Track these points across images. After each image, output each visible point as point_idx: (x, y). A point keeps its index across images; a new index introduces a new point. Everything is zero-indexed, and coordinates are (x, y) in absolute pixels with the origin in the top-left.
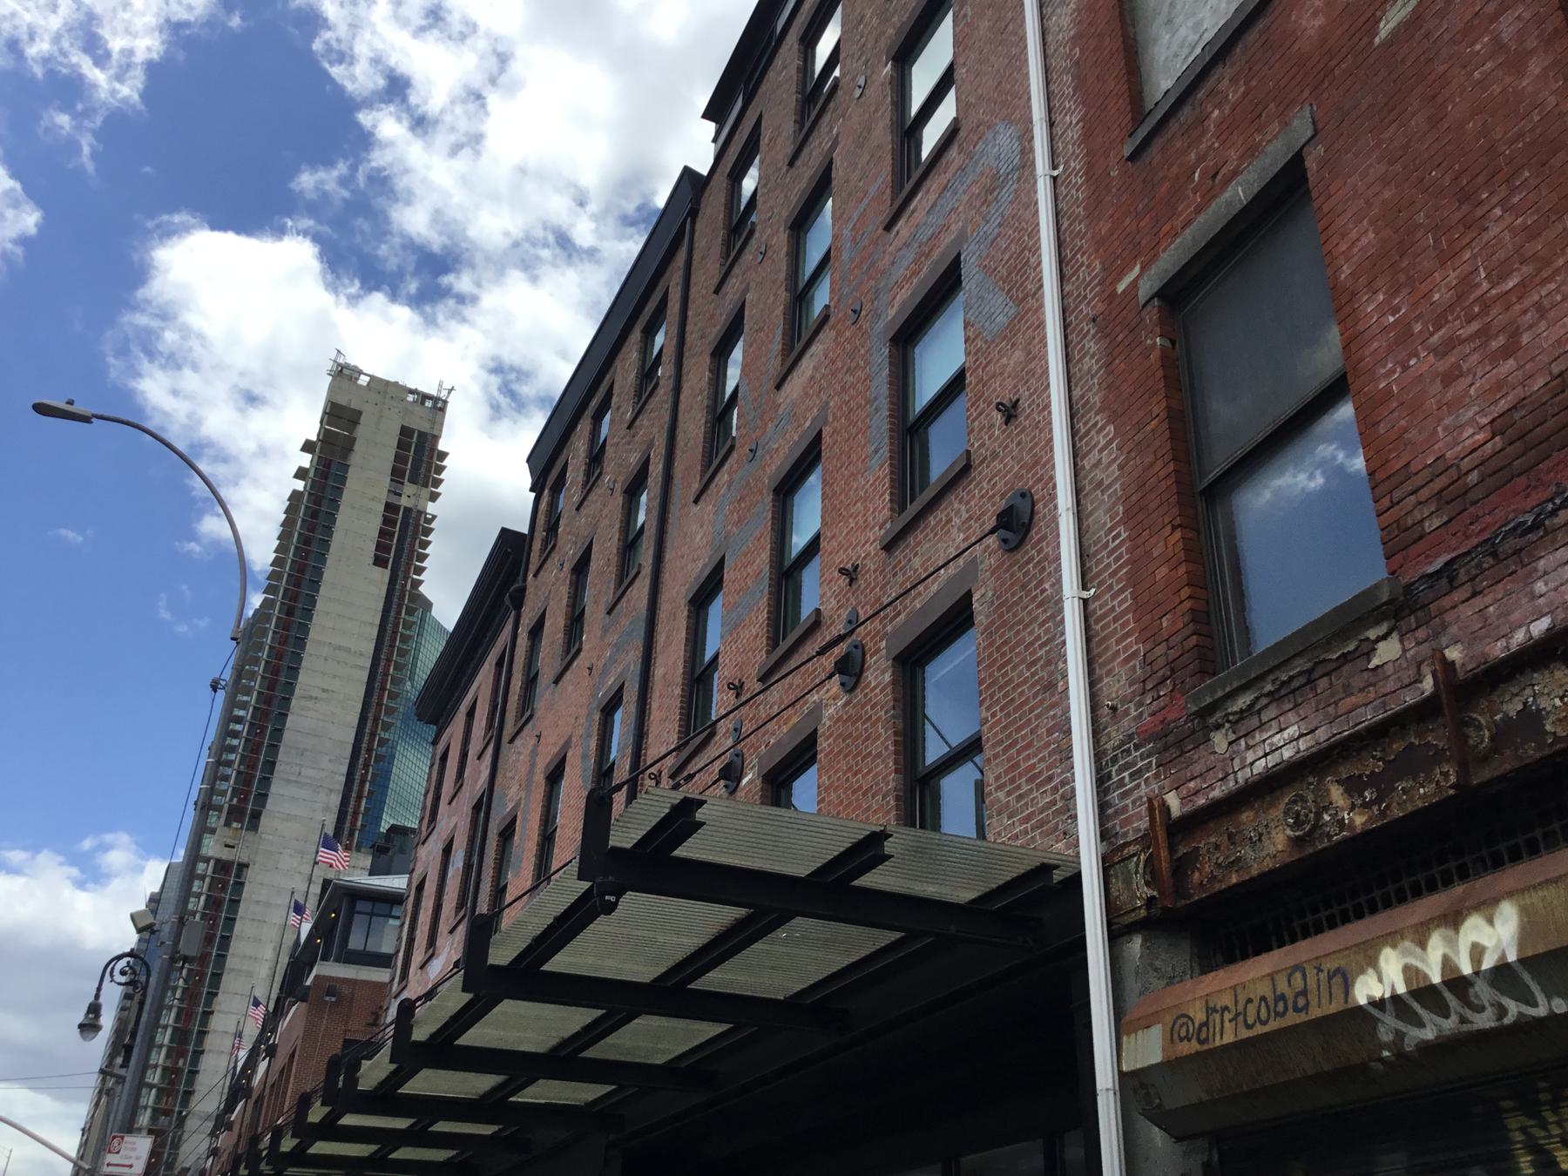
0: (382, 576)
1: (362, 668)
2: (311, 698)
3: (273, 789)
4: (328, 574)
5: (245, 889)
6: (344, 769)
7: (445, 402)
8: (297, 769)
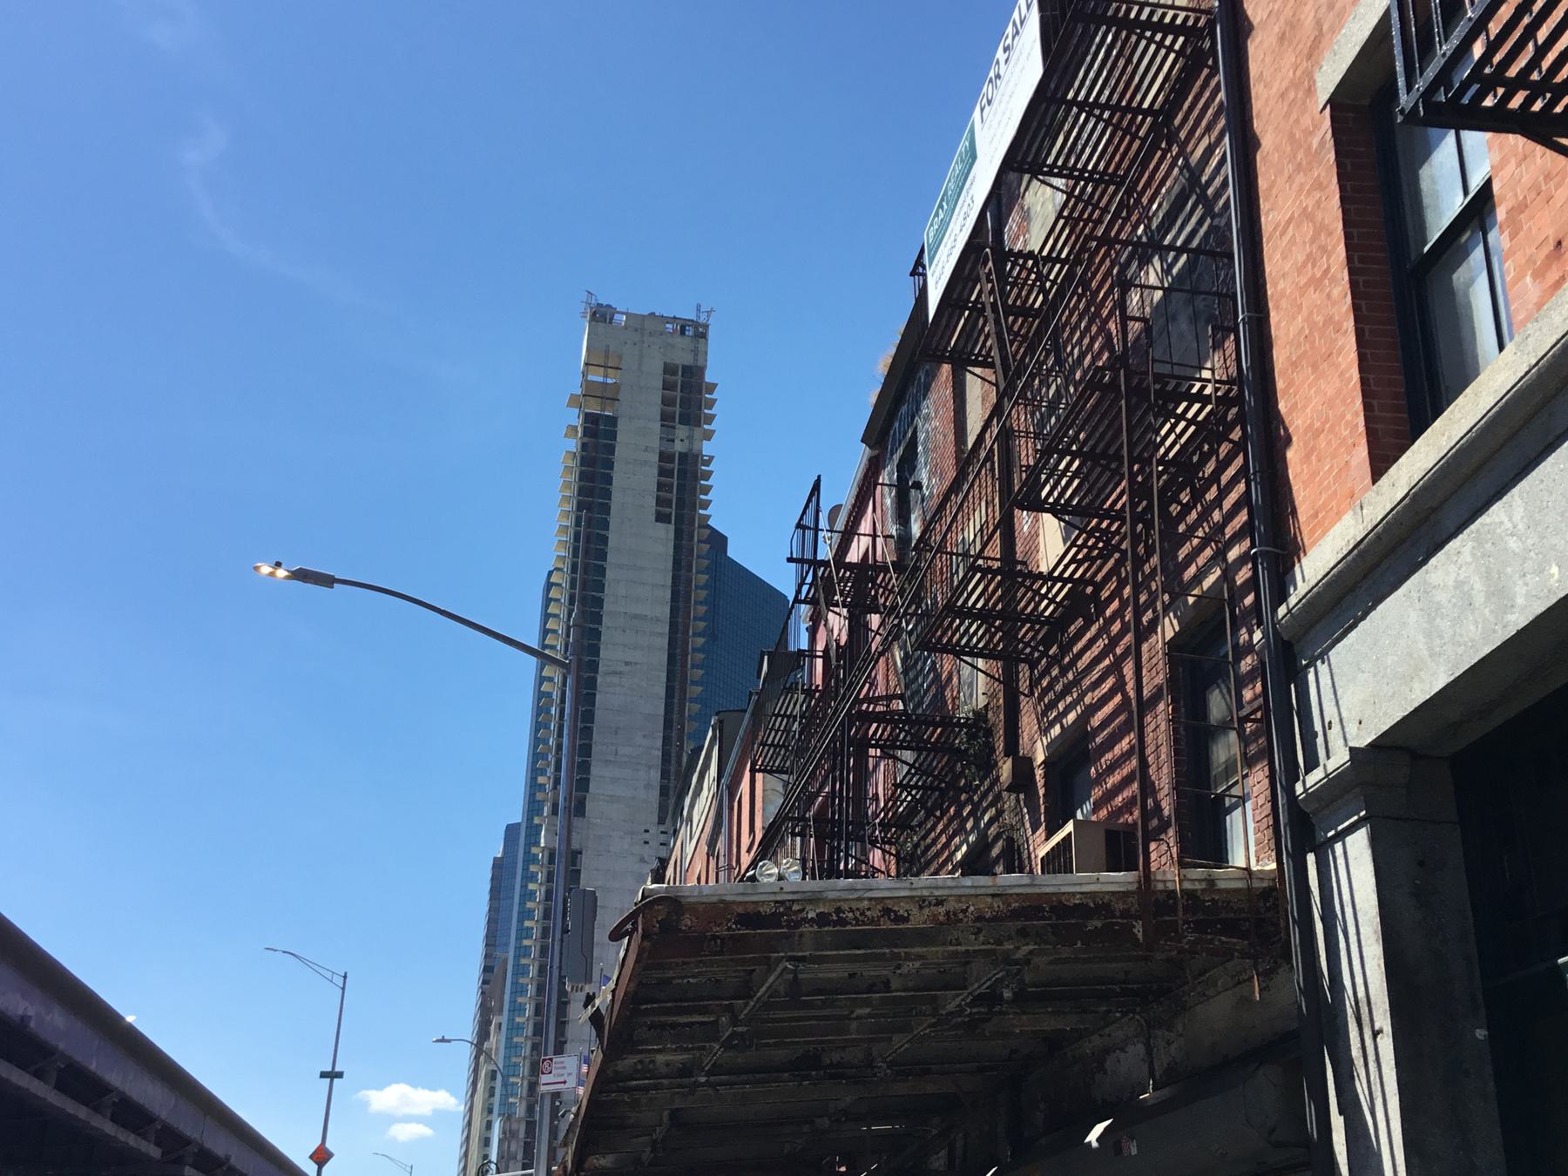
0: (666, 532)
1: (661, 634)
2: (616, 673)
3: (594, 770)
5: (582, 876)
6: (659, 743)
7: (706, 326)
8: (614, 748)
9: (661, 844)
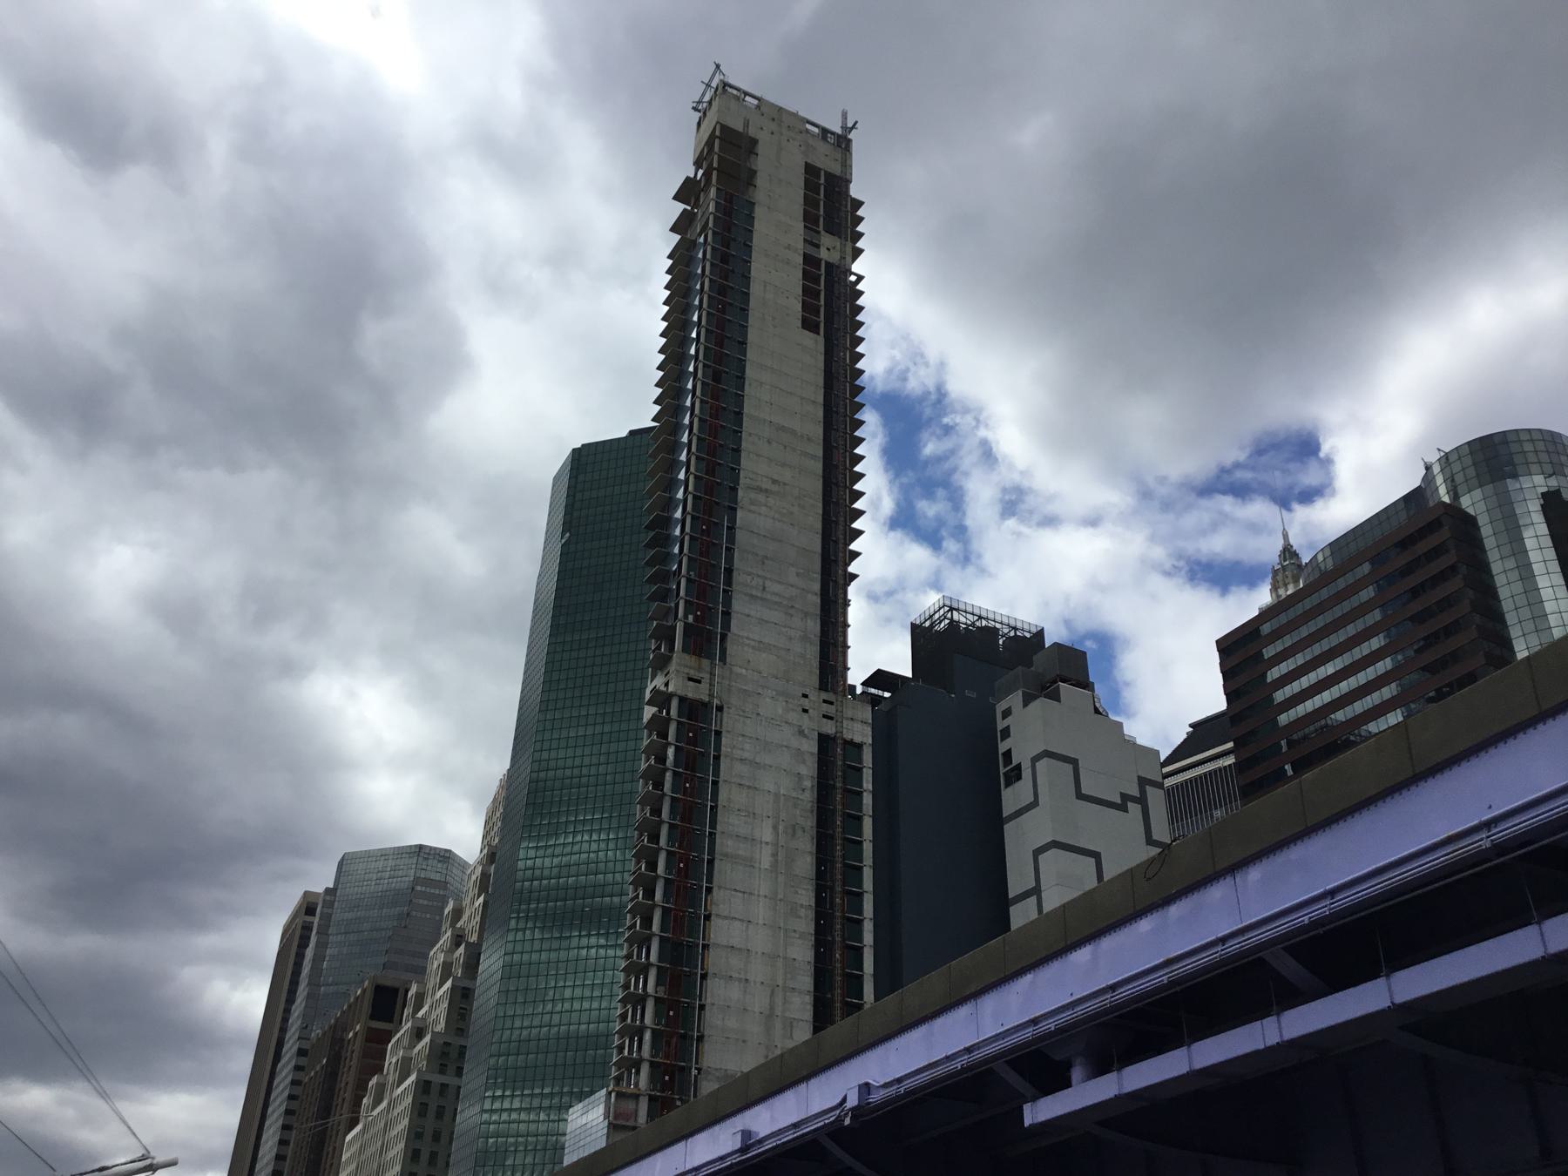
1: (814, 457)
2: (760, 490)
4: (753, 336)
9: (824, 716)
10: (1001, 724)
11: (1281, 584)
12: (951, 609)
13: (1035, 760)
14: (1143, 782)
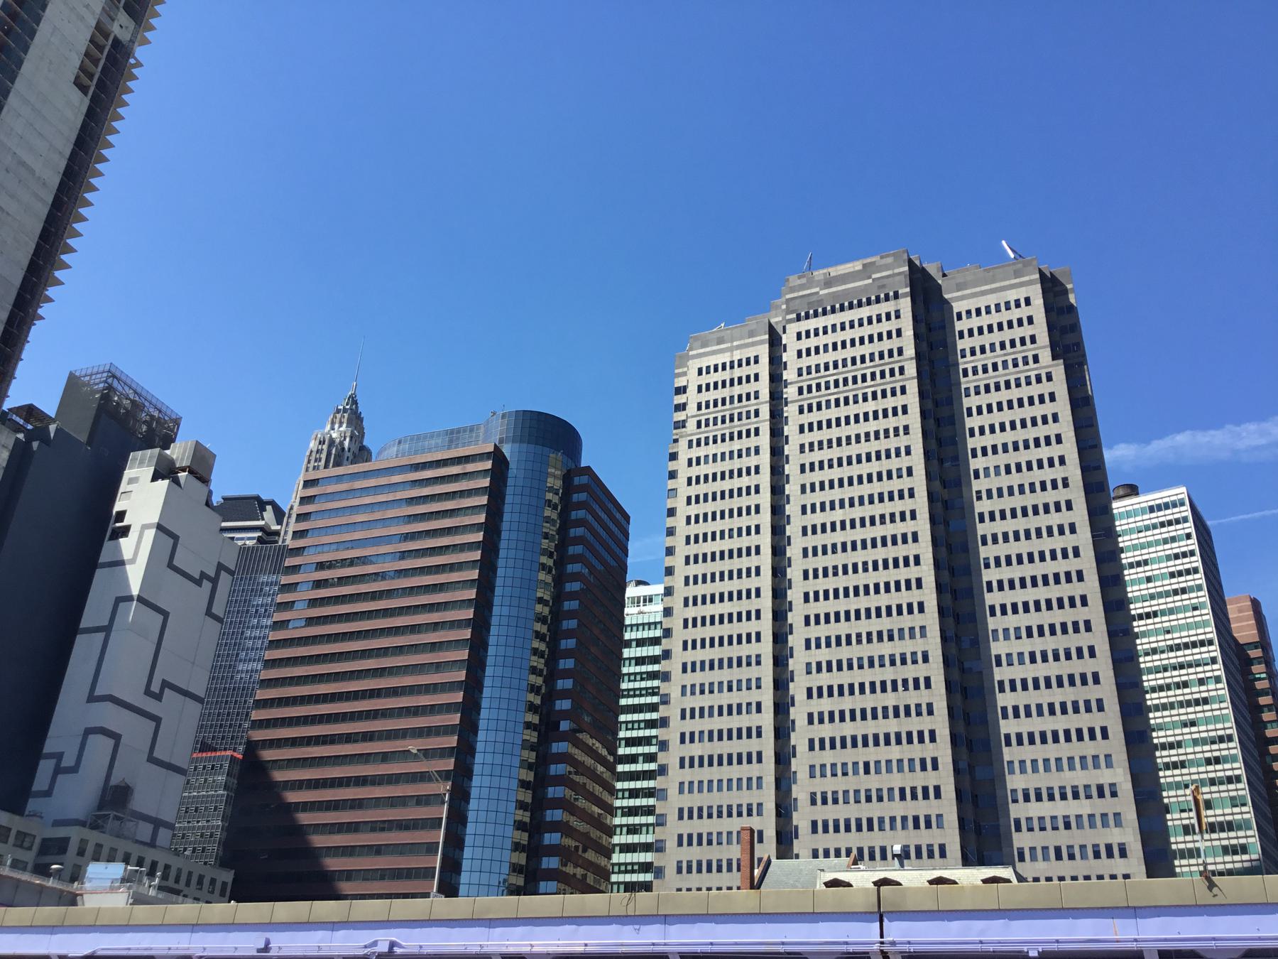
1: (42, 200)
10: (124, 486)
11: (338, 420)
12: (114, 376)
13: (145, 527)
14: (221, 567)
